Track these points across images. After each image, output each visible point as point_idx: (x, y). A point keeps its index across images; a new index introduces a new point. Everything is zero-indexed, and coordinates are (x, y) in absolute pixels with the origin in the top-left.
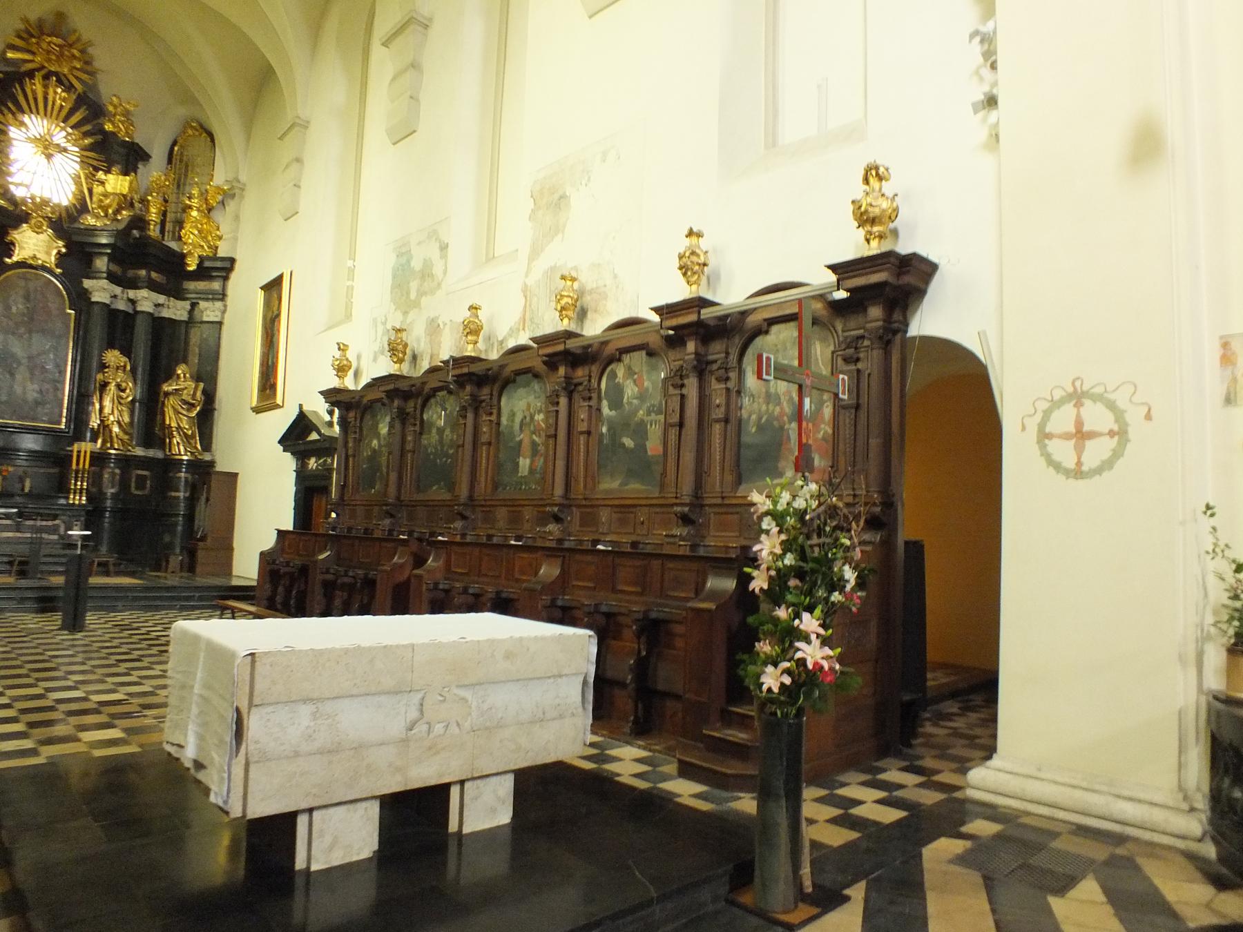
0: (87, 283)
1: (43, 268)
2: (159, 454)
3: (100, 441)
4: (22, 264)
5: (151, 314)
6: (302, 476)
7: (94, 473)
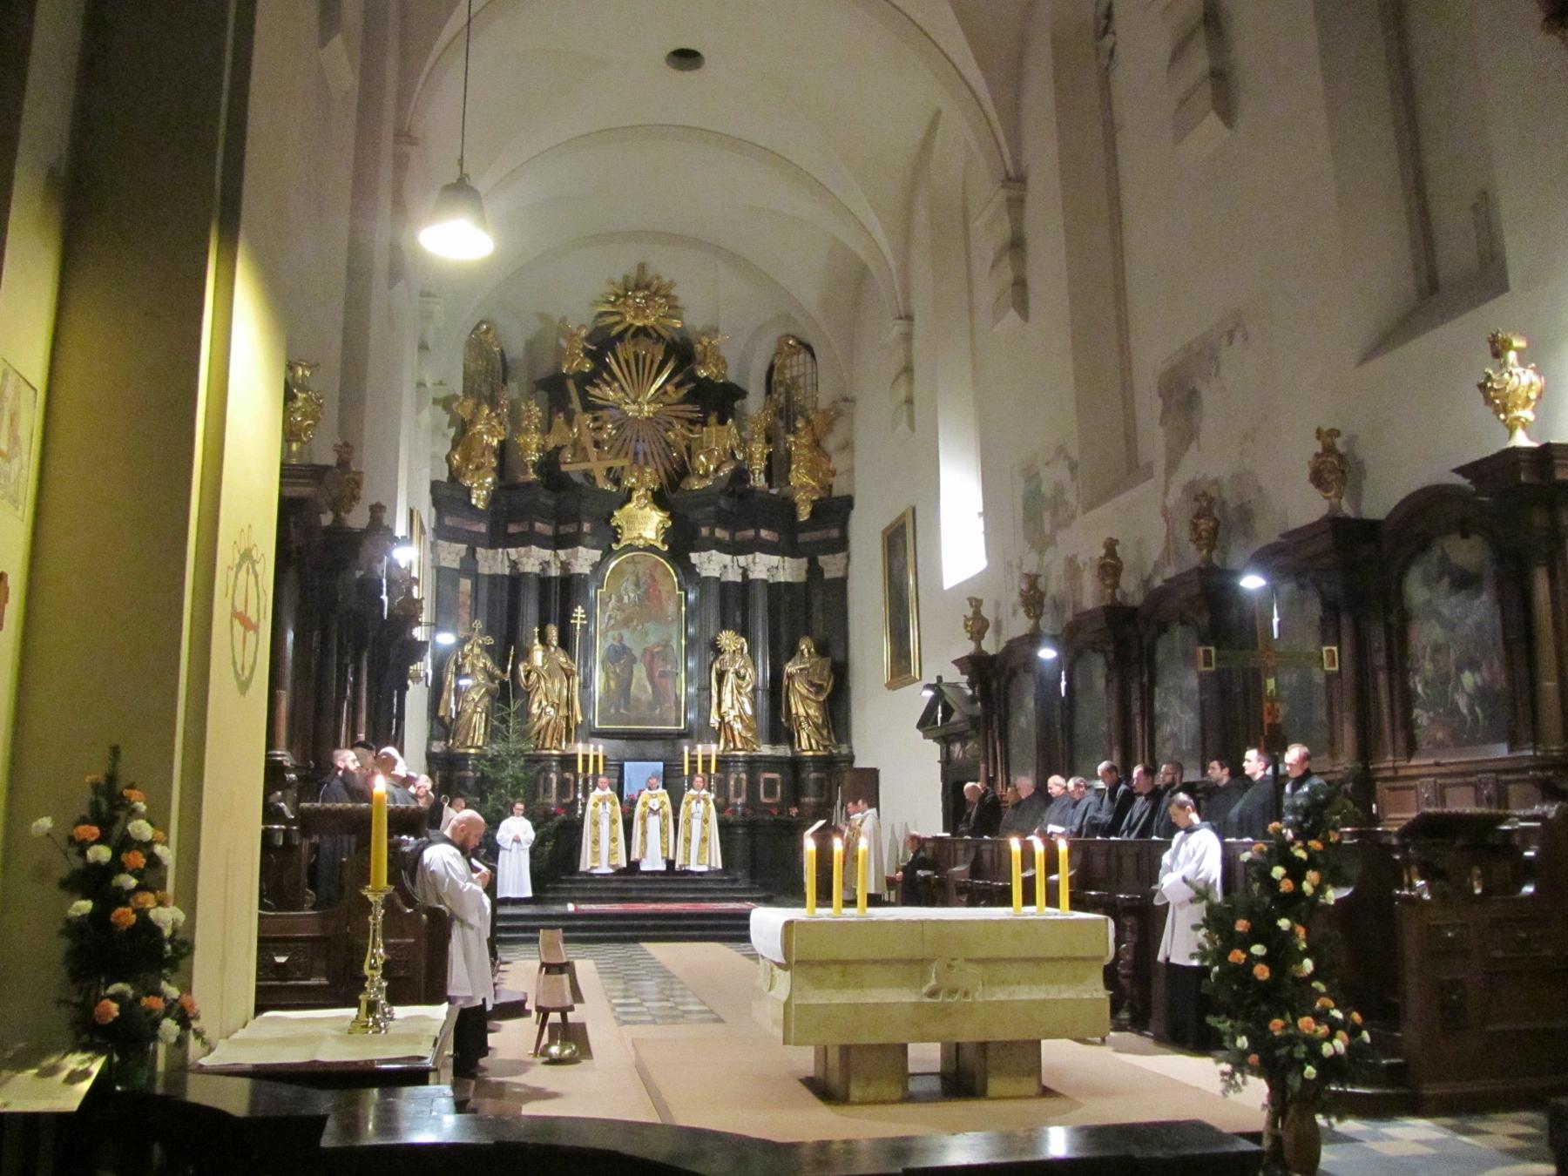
2: (783, 751)
5: (765, 581)
6: (946, 761)
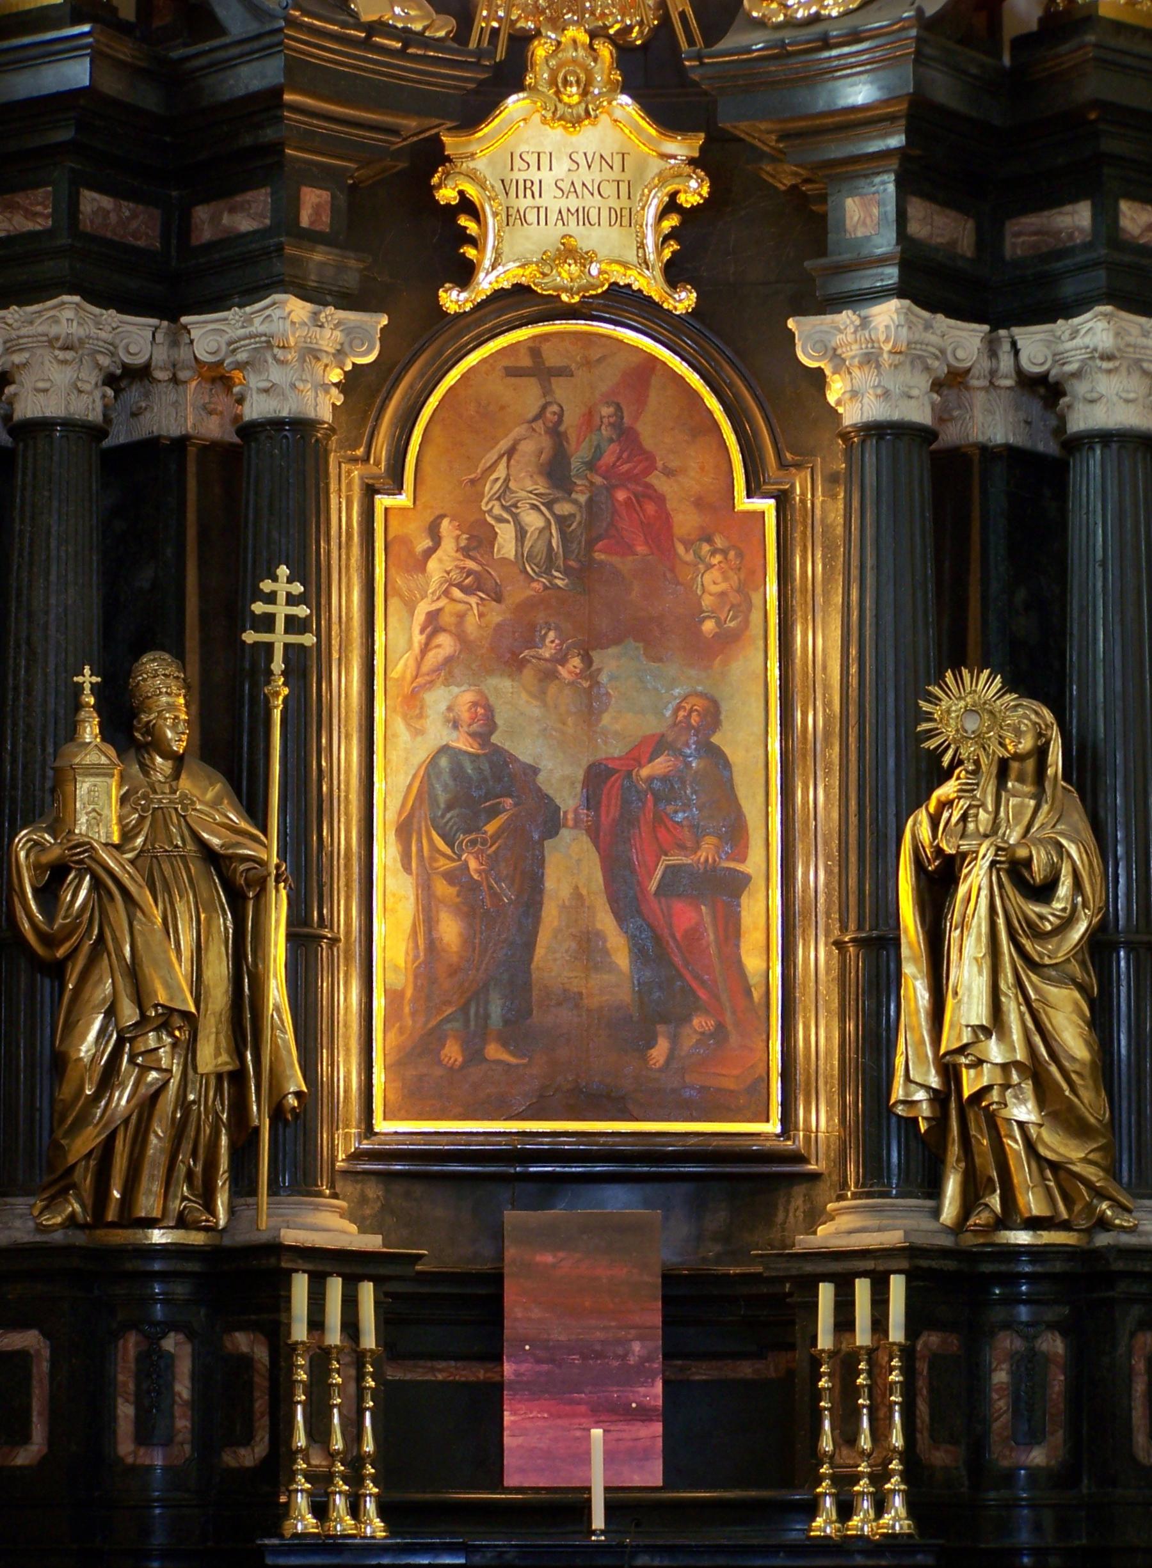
0: (811, 338)
1: (621, 302)
3: (952, 1187)
4: (518, 302)
7: (935, 1360)
